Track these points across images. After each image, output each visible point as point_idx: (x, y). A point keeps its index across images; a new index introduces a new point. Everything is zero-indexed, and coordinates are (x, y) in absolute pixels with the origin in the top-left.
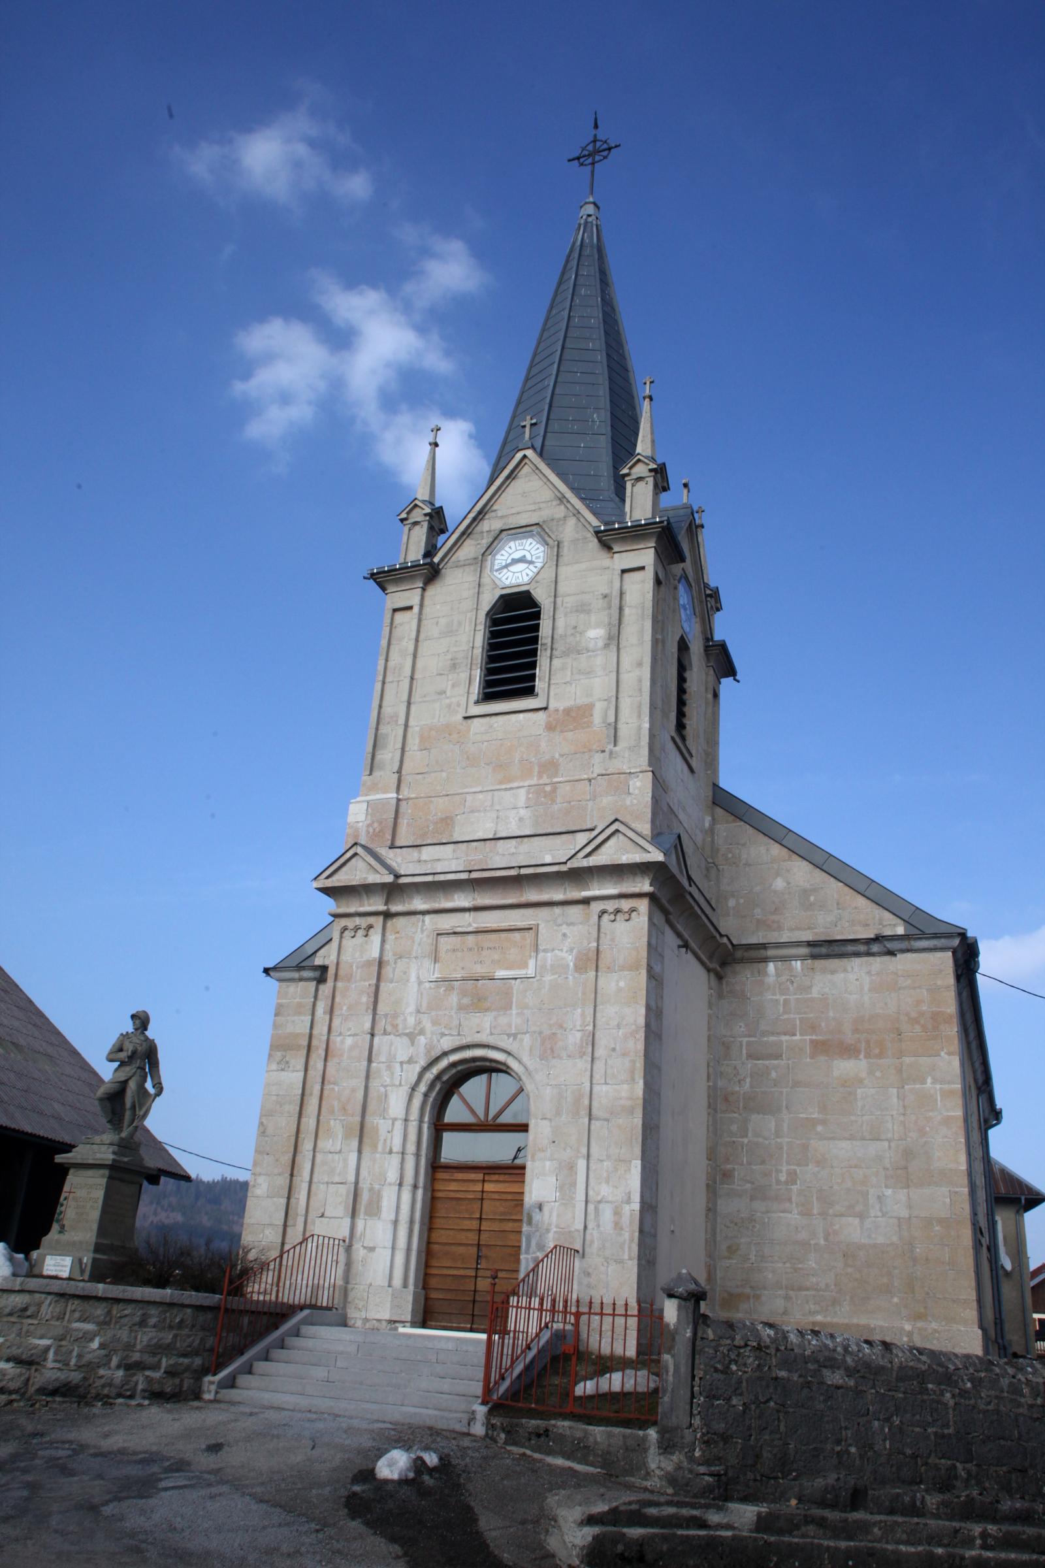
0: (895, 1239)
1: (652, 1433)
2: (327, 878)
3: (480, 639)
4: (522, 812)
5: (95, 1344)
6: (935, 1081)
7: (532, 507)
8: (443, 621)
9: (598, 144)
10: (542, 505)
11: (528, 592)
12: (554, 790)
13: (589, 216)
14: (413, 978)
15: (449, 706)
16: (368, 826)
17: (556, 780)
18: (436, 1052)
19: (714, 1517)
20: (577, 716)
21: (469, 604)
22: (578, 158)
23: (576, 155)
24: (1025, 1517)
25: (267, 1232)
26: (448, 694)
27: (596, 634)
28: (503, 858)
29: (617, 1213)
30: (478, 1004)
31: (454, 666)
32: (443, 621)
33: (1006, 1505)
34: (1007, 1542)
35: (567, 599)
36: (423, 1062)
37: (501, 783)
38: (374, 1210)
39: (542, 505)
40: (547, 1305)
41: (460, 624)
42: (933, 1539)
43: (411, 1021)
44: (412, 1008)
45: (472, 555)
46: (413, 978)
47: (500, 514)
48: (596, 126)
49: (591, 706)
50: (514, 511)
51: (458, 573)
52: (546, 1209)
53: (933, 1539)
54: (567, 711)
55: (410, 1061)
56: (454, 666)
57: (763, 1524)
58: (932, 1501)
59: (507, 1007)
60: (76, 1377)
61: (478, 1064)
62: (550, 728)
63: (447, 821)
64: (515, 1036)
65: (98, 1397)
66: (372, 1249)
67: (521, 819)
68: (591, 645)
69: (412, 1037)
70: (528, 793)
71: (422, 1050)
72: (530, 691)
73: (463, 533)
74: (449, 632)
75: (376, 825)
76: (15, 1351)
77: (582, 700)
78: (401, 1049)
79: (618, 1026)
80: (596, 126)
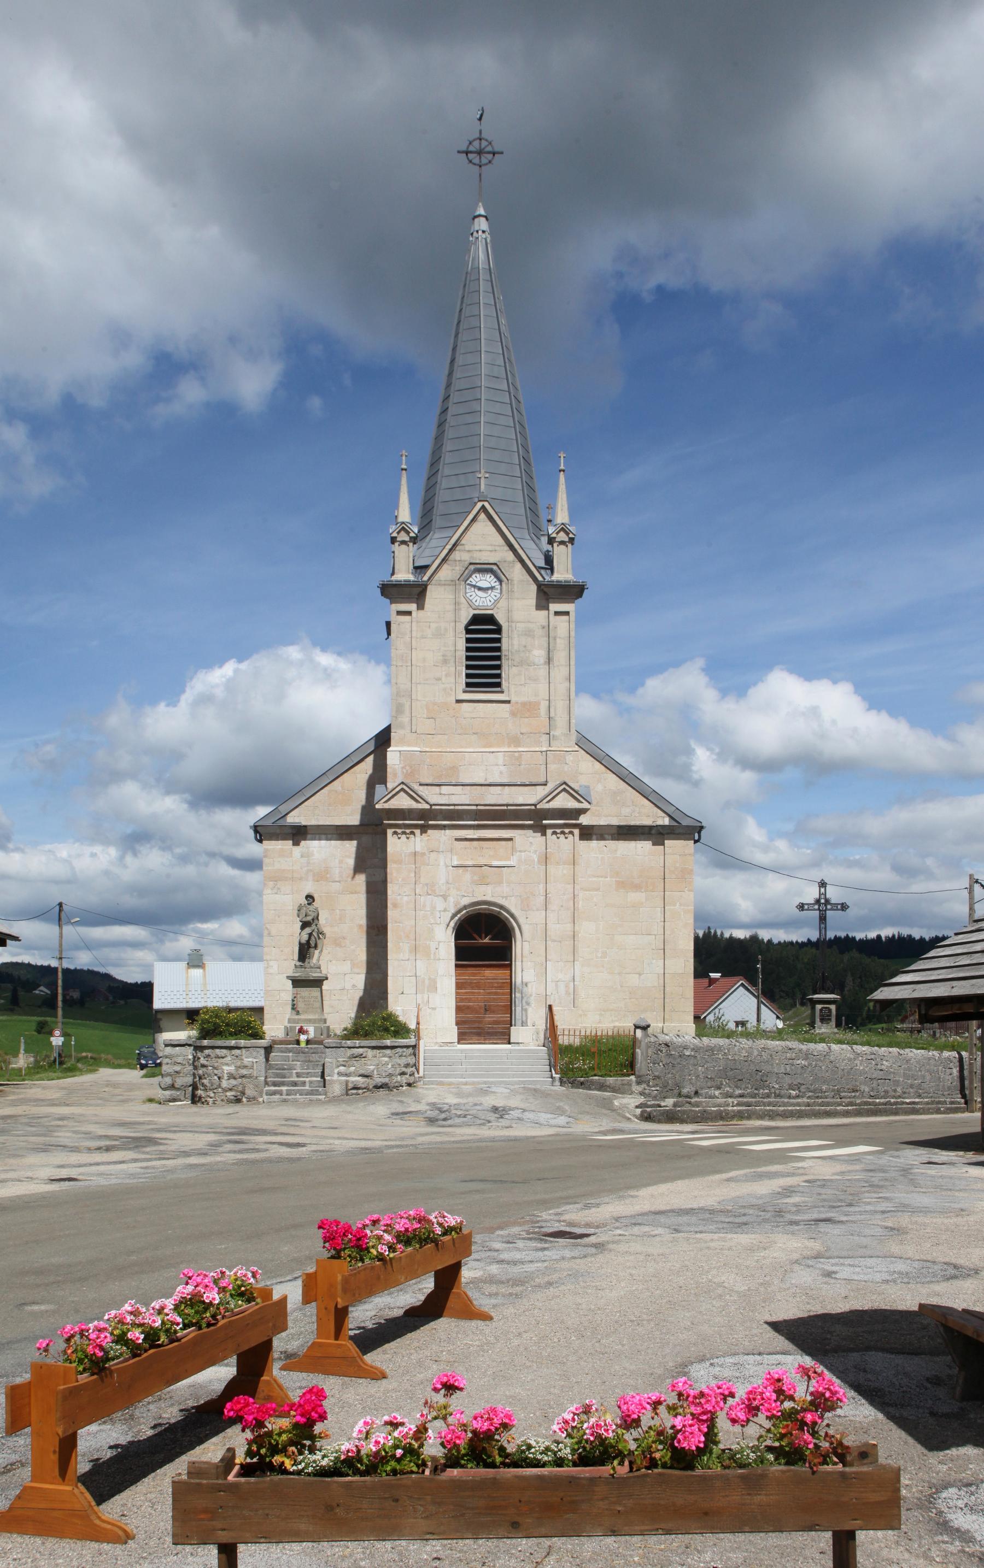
0: (656, 984)
1: (633, 1077)
2: (386, 802)
3: (462, 644)
4: (502, 768)
5: (390, 1066)
6: (681, 905)
7: (490, 548)
8: (433, 626)
9: (484, 143)
10: (497, 548)
11: (492, 615)
12: (520, 756)
13: (484, 232)
14: (442, 863)
15: (445, 690)
16: (403, 768)
17: (520, 749)
18: (459, 907)
19: (663, 1104)
20: (529, 708)
21: (450, 616)
22: (467, 153)
23: (464, 148)
24: (741, 1096)
25: (282, 995)
26: (443, 679)
27: (539, 654)
28: (495, 797)
29: (567, 986)
30: (483, 882)
31: (445, 662)
32: (433, 626)
33: (738, 1092)
34: (738, 1105)
35: (518, 625)
36: (453, 911)
37: (485, 747)
38: (433, 988)
39: (497, 548)
40: (572, 1033)
41: (446, 630)
42: (719, 1106)
43: (444, 888)
44: (443, 881)
45: (449, 578)
46: (442, 863)
47: (467, 548)
48: (480, 119)
49: (538, 704)
50: (477, 548)
51: (441, 589)
52: (529, 985)
53: (719, 1106)
54: (524, 704)
55: (445, 910)
56: (445, 662)
57: (675, 1105)
58: (717, 1093)
59: (500, 882)
60: (386, 1080)
61: (511, 920)
62: (513, 714)
63: (454, 769)
64: (506, 897)
65: (395, 1087)
66: (434, 1009)
67: (501, 773)
68: (536, 660)
69: (445, 897)
70: (504, 756)
71: (452, 905)
72: (499, 685)
73: (443, 560)
74: (439, 634)
75: (408, 768)
76: (362, 1072)
77: (532, 699)
78: (440, 904)
79: (564, 894)
80: (480, 119)
